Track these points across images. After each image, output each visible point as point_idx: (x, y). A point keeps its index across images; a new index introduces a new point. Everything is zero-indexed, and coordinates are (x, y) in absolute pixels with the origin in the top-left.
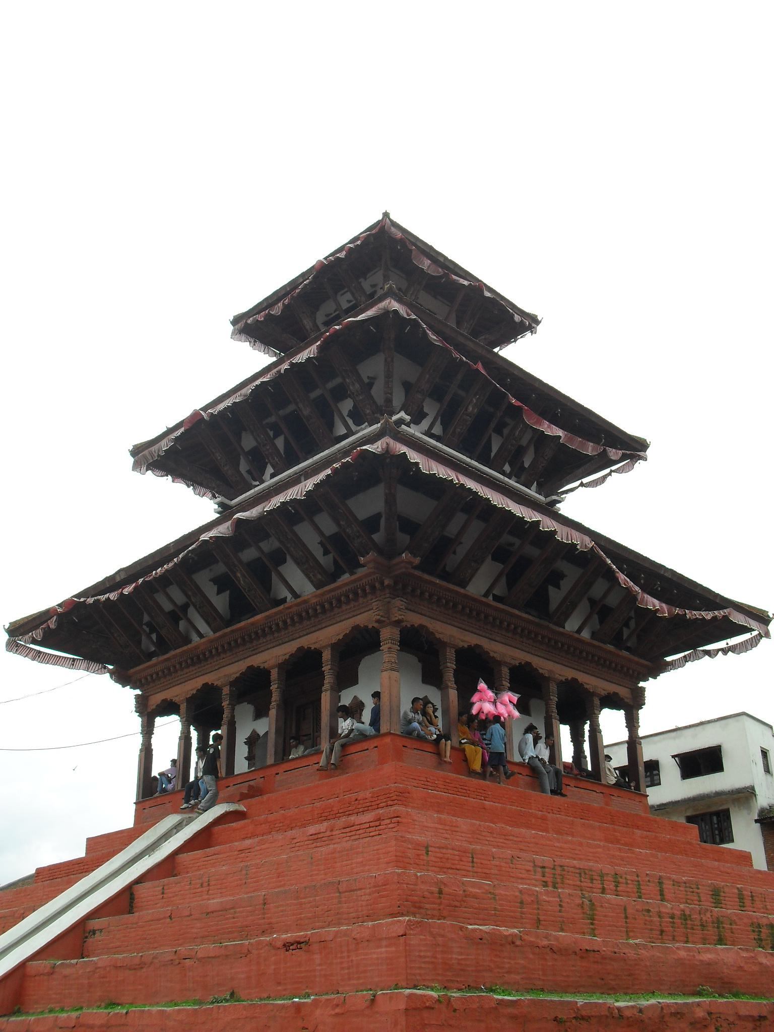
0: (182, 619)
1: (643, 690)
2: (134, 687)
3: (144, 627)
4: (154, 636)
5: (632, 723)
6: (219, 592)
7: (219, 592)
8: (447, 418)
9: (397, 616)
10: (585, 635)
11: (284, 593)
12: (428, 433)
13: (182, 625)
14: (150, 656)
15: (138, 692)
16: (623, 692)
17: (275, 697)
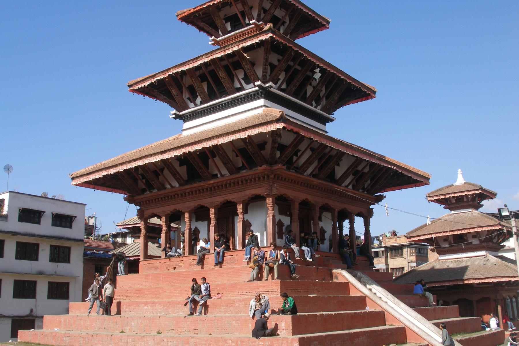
0: (160, 175)
1: (372, 209)
2: (136, 205)
3: (139, 176)
4: (144, 181)
5: (367, 224)
6: (181, 165)
7: (181, 165)
8: (289, 81)
9: (275, 192)
10: (350, 187)
11: (216, 172)
12: (279, 89)
13: (161, 177)
14: (144, 191)
15: (138, 208)
16: (364, 211)
17: (213, 221)
